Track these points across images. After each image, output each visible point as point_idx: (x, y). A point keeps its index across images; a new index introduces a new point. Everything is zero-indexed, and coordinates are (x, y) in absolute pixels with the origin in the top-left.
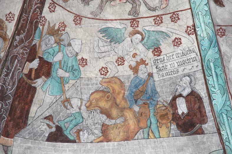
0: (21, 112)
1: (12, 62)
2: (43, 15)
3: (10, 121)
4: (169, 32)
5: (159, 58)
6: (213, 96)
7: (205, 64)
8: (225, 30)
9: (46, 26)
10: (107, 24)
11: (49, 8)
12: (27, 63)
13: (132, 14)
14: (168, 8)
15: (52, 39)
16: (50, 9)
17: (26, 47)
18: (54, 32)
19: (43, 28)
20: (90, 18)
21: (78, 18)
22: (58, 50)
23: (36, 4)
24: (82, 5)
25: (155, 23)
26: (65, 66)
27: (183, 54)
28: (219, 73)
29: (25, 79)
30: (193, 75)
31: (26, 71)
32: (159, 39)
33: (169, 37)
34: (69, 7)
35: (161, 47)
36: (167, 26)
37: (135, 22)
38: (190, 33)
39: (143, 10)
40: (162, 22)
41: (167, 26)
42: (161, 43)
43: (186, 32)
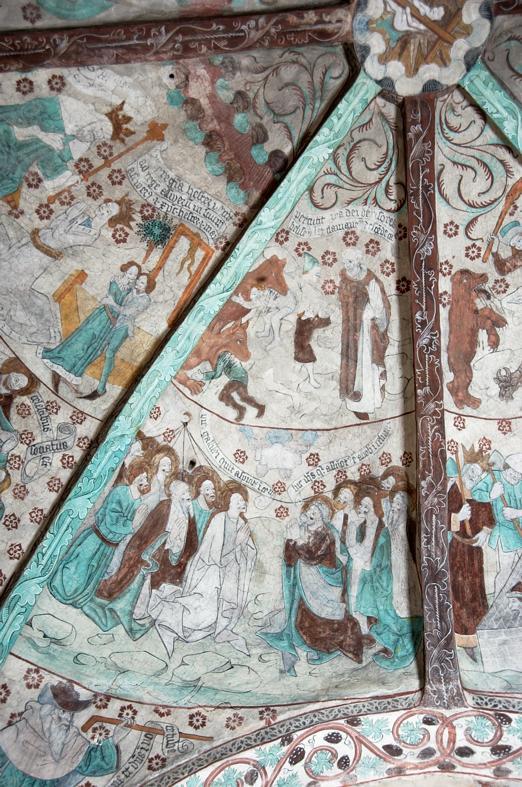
0: (472, 590)
1: (429, 521)
2: (448, 439)
3: (461, 608)
9: (461, 453)
12: (453, 514)
15: (477, 467)
17: (440, 492)
18: (474, 457)
19: (457, 457)
21: (504, 423)
22: (492, 481)
23: (432, 427)
24: (503, 402)
26: (513, 501)
29: (459, 539)
31: (456, 527)
34: (485, 413)
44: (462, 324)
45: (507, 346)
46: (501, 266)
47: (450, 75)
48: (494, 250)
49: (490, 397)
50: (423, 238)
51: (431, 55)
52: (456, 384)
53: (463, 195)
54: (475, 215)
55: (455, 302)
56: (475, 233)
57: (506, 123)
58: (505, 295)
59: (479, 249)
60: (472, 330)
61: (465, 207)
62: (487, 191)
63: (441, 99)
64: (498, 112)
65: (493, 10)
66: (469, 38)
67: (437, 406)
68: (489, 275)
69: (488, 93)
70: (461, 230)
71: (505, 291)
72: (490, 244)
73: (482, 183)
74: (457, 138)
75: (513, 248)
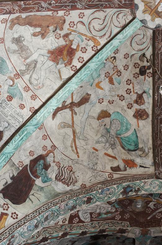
4: (24, 98)
5: (7, 101)
6: (10, 144)
7: (23, 129)
8: (42, 128)
10: (7, 60)
11: (3, 19)
13: (21, 72)
14: (36, 90)
16: (3, 20)
20: (5, 47)
21: (2, 40)
24: (11, 40)
25: (24, 88)
27: (18, 114)
28: (24, 139)
30: (11, 126)
32: (17, 95)
33: (22, 101)
35: (14, 99)
36: (27, 95)
37: (18, 76)
38: (31, 110)
39: (26, 77)
40: (27, 92)
41: (27, 95)
42: (16, 98)
43: (30, 108)
44: (44, 21)
45: (34, 40)
46: (66, 36)
47: (139, 14)
48: (72, 33)
49: (13, 34)
50: (84, 4)
51: (147, 7)
52: (20, 19)
53: (94, 20)
54: (86, 25)
55: (53, 17)
56: (80, 25)
57: (122, 35)
58: (54, 38)
59: (73, 27)
60: (41, 25)
61: (89, 21)
62: (95, 30)
63: (129, 11)
64: (126, 32)
65: (158, 28)
66: (151, 21)
67: (17, 11)
68: (63, 31)
69: (133, 28)
70: (81, 20)
71: (56, 38)
72: (75, 31)
73: (98, 27)
74: (115, 17)
75: (73, 40)
